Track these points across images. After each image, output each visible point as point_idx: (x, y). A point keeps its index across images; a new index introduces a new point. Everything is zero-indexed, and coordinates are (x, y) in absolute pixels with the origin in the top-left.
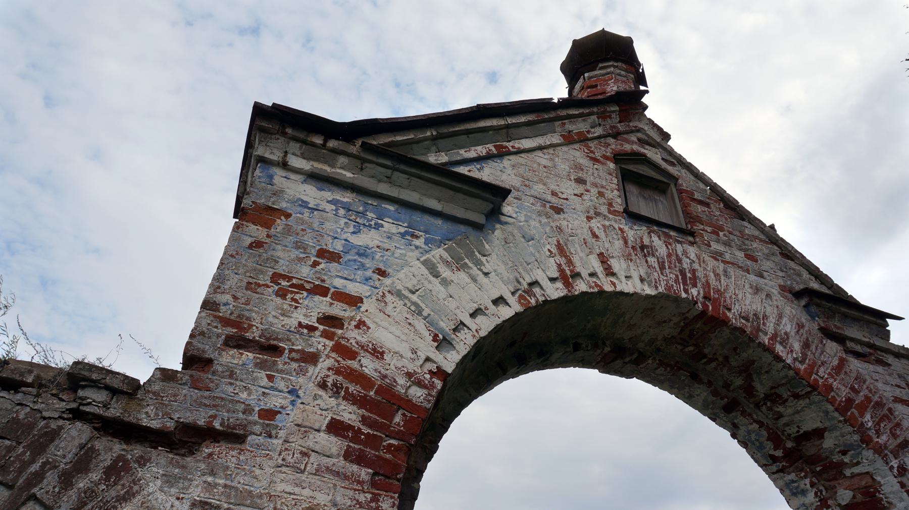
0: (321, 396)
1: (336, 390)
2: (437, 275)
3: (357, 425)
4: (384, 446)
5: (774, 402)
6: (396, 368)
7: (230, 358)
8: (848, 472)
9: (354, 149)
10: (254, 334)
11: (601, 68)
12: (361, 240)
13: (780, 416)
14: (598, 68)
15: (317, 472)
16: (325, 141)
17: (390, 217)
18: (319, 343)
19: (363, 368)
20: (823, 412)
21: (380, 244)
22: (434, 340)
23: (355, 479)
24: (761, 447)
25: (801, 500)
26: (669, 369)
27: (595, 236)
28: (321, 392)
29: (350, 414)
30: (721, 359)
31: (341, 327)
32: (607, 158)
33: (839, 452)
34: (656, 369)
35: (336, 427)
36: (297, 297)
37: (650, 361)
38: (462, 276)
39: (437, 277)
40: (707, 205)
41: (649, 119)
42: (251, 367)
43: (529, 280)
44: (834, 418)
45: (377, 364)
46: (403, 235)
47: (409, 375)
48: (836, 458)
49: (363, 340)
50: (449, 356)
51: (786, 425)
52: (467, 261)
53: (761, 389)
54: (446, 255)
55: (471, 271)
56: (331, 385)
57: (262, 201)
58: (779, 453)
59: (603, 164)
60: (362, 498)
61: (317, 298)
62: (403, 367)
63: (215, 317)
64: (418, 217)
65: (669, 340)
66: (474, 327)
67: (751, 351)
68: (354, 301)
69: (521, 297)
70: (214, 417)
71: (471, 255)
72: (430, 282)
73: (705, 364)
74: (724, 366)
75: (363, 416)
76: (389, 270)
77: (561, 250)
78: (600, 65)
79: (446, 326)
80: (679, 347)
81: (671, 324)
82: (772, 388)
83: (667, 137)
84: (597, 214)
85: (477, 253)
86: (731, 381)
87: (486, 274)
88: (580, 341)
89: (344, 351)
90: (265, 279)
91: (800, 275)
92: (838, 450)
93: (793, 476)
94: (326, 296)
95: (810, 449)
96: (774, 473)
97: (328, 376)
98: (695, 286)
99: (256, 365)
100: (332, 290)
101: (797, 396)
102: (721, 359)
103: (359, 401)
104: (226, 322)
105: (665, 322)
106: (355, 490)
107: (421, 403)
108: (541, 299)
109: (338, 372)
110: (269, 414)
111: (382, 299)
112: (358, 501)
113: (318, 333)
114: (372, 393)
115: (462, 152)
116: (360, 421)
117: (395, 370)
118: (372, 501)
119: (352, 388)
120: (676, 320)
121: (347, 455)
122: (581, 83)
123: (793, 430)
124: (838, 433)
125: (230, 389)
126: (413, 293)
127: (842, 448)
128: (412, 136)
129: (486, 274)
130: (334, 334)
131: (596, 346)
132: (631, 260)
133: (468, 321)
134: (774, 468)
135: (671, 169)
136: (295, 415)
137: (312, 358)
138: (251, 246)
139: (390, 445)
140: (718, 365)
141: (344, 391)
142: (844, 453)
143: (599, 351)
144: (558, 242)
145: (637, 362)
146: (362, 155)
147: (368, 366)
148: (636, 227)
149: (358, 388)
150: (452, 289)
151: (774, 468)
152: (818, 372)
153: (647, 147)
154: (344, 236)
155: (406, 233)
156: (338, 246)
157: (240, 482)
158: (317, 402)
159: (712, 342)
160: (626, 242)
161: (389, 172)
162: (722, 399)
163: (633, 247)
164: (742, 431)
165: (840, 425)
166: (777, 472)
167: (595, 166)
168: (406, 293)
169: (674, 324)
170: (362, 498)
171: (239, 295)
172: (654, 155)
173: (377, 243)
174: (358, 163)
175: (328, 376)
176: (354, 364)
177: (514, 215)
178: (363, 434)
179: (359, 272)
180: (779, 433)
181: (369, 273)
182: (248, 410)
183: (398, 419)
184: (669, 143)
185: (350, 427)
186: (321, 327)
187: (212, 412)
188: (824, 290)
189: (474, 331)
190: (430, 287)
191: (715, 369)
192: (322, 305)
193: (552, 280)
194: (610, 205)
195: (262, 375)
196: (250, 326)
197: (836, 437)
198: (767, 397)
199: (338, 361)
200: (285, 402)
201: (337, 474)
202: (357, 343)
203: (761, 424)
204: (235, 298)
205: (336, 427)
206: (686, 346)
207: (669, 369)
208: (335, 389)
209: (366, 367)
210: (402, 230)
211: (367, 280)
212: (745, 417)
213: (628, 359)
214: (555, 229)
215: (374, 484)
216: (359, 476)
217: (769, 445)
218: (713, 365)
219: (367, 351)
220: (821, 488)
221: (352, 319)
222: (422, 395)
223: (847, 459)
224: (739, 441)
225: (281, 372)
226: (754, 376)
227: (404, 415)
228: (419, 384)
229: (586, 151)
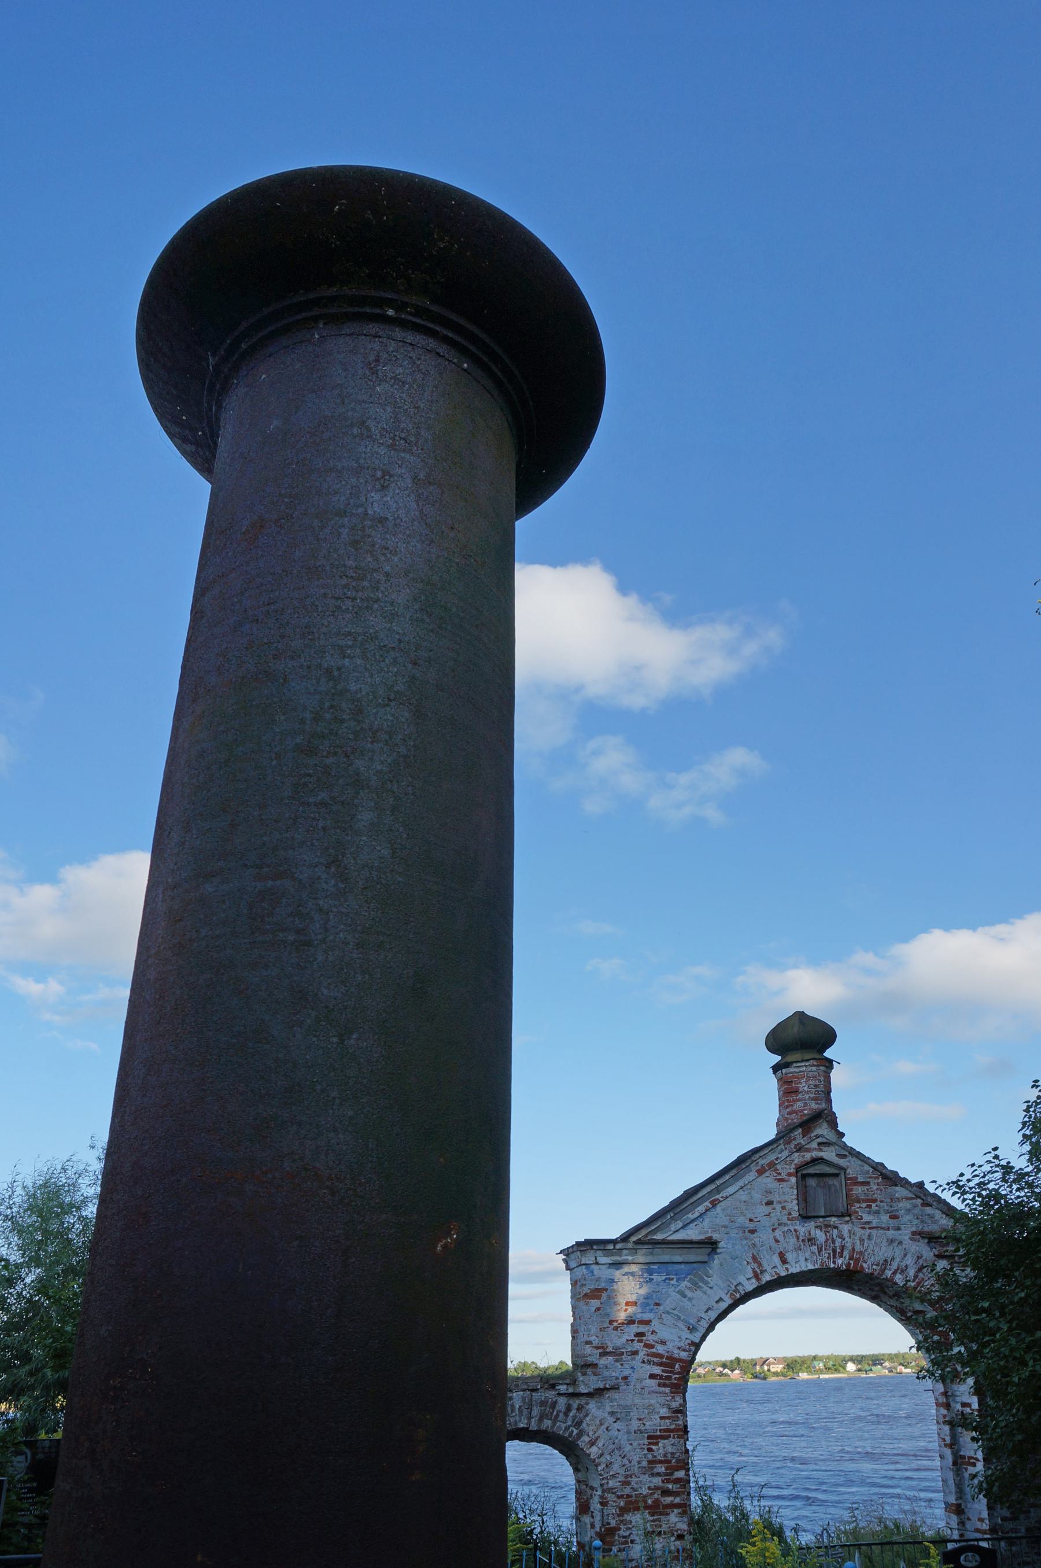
1: (649, 1362)
2: (685, 1296)
3: (661, 1373)
7: (603, 1361)
9: (630, 1245)
10: (610, 1349)
15: (649, 1393)
16: (614, 1246)
18: (637, 1346)
22: (688, 1329)
27: (777, 1241)
28: (643, 1365)
29: (657, 1370)
31: (645, 1336)
32: (789, 1174)
35: (652, 1376)
36: (622, 1328)
38: (699, 1293)
39: (685, 1298)
42: (613, 1363)
43: (735, 1284)
45: (665, 1347)
46: (664, 1281)
47: (679, 1348)
49: (656, 1339)
50: (696, 1335)
52: (700, 1284)
54: (689, 1284)
55: (703, 1289)
57: (593, 1287)
60: (668, 1398)
61: (632, 1326)
63: (593, 1347)
64: (670, 1267)
66: (707, 1318)
68: (648, 1322)
69: (731, 1294)
70: (605, 1384)
71: (702, 1280)
72: (682, 1302)
76: (661, 1302)
77: (755, 1259)
79: (693, 1321)
85: (705, 1278)
87: (711, 1288)
89: (647, 1346)
90: (606, 1325)
94: (634, 1324)
99: (615, 1361)
100: (637, 1320)
103: (661, 1364)
104: (597, 1348)
108: (743, 1293)
109: (648, 1355)
110: (625, 1378)
111: (660, 1318)
113: (636, 1342)
114: (664, 1360)
115: (690, 1215)
119: (656, 1360)
121: (659, 1385)
125: (607, 1373)
126: (674, 1310)
128: (660, 1223)
129: (711, 1288)
130: (642, 1340)
133: (703, 1315)
136: (635, 1376)
137: (636, 1353)
138: (595, 1311)
144: (753, 1254)
146: (636, 1247)
147: (660, 1349)
148: (806, 1225)
149: (658, 1359)
150: (694, 1302)
154: (636, 1292)
155: (666, 1279)
157: (622, 1402)
160: (798, 1238)
161: (651, 1250)
163: (803, 1241)
167: (781, 1186)
168: (671, 1311)
170: (668, 1398)
171: (598, 1335)
173: (652, 1289)
174: (634, 1251)
176: (654, 1350)
177: (725, 1246)
179: (647, 1308)
181: (652, 1307)
182: (617, 1378)
183: (677, 1366)
186: (636, 1339)
187: (604, 1382)
190: (682, 1304)
192: (634, 1329)
195: (618, 1364)
196: (607, 1347)
200: (630, 1372)
201: (657, 1392)
204: (597, 1337)
205: (652, 1376)
210: (664, 1278)
211: (651, 1310)
215: (671, 1392)
221: (648, 1331)
225: (625, 1361)
228: (684, 1350)
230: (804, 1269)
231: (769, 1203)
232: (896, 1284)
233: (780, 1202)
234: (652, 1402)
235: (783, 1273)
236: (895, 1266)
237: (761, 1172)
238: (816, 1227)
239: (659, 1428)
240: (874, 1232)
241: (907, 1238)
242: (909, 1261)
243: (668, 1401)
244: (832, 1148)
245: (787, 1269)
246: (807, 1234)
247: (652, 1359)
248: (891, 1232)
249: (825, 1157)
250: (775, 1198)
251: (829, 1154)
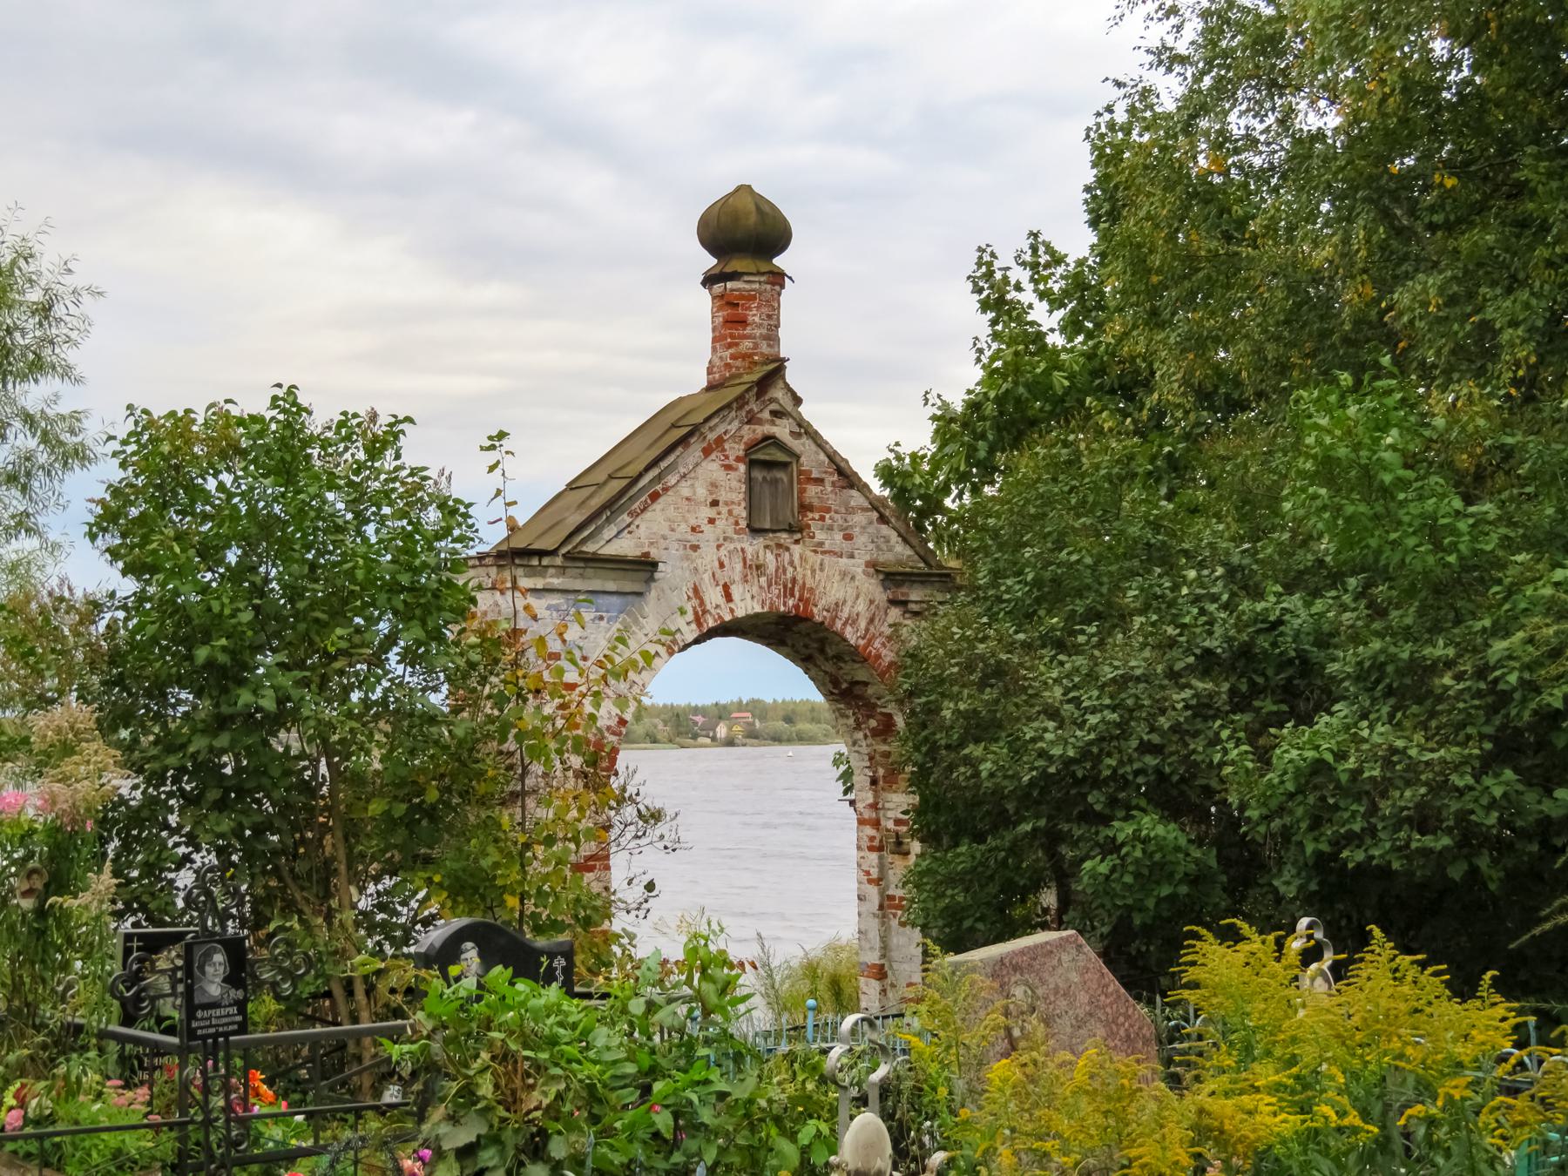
24: (824, 684)
27: (722, 565)
77: (696, 590)
198: (834, 657)
230: (750, 612)
231: (715, 503)
232: (845, 640)
233: (726, 504)
235: (728, 618)
236: (845, 615)
237: (707, 452)
238: (767, 547)
240: (827, 558)
241: (860, 570)
242: (861, 607)
244: (784, 421)
245: (732, 611)
248: (844, 561)
250: (723, 496)
251: (782, 430)
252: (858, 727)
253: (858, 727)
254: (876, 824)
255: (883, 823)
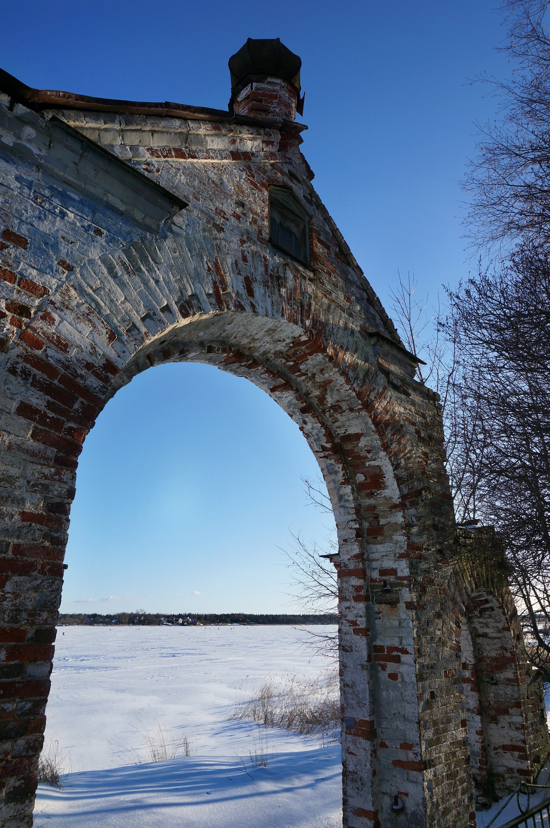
0: (11, 382)
4: (65, 429)
5: (335, 411)
6: (77, 360)
8: (367, 464)
11: (269, 83)
12: (45, 227)
13: (336, 421)
14: (266, 82)
17: (74, 207)
19: (49, 358)
20: (365, 423)
21: (65, 235)
23: (41, 456)
24: (317, 440)
25: (333, 477)
26: (272, 376)
27: (245, 259)
28: (12, 378)
30: (309, 375)
33: (366, 450)
34: (263, 374)
37: (260, 368)
40: (328, 247)
41: (301, 154)
44: (370, 428)
46: (87, 229)
48: (363, 454)
51: (338, 427)
53: (330, 400)
56: (20, 371)
58: (328, 445)
59: (260, 190)
60: (46, 471)
62: (83, 360)
65: (278, 354)
67: (332, 374)
73: (298, 376)
74: (310, 380)
75: (48, 402)
78: (269, 79)
80: (284, 361)
81: (284, 344)
82: (338, 401)
83: (311, 175)
84: (249, 239)
85: (150, 259)
86: (311, 391)
88: (214, 345)
91: (375, 319)
92: (366, 449)
93: (333, 461)
95: (348, 447)
96: (321, 458)
97: (17, 363)
98: (308, 318)
101: (351, 410)
102: (309, 375)
103: (46, 389)
105: (280, 341)
106: (42, 465)
107: (97, 393)
112: (44, 474)
116: (45, 406)
117: (75, 361)
118: (56, 474)
120: (288, 341)
122: (247, 91)
123: (341, 431)
124: (369, 438)
127: (369, 448)
131: (224, 351)
132: (268, 287)
134: (322, 454)
135: (308, 207)
139: (71, 428)
140: (307, 378)
141: (32, 378)
142: (369, 452)
143: (225, 355)
145: (249, 367)
151: (322, 454)
152: (369, 395)
153: (294, 181)
156: (24, 230)
158: (7, 386)
159: (308, 362)
162: (302, 403)
164: (308, 427)
165: (373, 433)
166: (323, 457)
169: (286, 344)
170: (46, 471)
172: (299, 191)
175: (17, 363)
176: (39, 352)
178: (48, 417)
180: (333, 432)
183: (76, 406)
184: (312, 182)
185: (37, 411)
188: (388, 336)
189: (143, 333)
191: (304, 381)
193: (208, 295)
194: (260, 232)
197: (367, 441)
198: (332, 407)
199: (26, 350)
202: (43, 333)
203: (323, 424)
206: (288, 361)
207: (272, 376)
208: (24, 376)
209: (50, 357)
212: (313, 418)
213: (242, 364)
214: (215, 247)
216: (45, 454)
217: (324, 439)
218: (303, 378)
219: (52, 342)
220: (348, 471)
222: (98, 387)
223: (369, 456)
224: (303, 433)
226: (328, 392)
227: (82, 402)
228: (97, 375)
229: (248, 174)
234: (14, 471)
239: (16, 541)
243: (46, 477)
246: (276, 270)
247: (35, 371)
249: (294, 190)
252: (347, 481)
253: (347, 481)
254: (362, 574)
255: (368, 573)
